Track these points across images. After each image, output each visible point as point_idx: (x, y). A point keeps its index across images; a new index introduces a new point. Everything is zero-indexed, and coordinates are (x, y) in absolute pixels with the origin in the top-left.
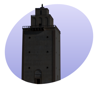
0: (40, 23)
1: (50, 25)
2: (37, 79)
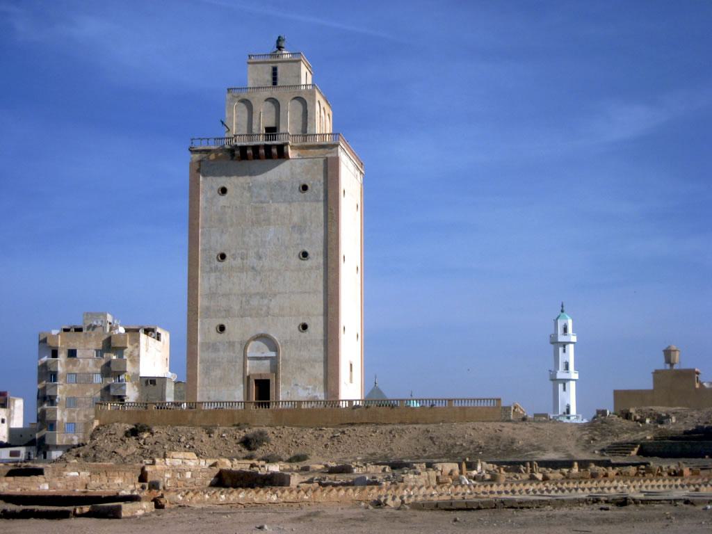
0: (271, 124)
1: (318, 131)
2: (257, 382)
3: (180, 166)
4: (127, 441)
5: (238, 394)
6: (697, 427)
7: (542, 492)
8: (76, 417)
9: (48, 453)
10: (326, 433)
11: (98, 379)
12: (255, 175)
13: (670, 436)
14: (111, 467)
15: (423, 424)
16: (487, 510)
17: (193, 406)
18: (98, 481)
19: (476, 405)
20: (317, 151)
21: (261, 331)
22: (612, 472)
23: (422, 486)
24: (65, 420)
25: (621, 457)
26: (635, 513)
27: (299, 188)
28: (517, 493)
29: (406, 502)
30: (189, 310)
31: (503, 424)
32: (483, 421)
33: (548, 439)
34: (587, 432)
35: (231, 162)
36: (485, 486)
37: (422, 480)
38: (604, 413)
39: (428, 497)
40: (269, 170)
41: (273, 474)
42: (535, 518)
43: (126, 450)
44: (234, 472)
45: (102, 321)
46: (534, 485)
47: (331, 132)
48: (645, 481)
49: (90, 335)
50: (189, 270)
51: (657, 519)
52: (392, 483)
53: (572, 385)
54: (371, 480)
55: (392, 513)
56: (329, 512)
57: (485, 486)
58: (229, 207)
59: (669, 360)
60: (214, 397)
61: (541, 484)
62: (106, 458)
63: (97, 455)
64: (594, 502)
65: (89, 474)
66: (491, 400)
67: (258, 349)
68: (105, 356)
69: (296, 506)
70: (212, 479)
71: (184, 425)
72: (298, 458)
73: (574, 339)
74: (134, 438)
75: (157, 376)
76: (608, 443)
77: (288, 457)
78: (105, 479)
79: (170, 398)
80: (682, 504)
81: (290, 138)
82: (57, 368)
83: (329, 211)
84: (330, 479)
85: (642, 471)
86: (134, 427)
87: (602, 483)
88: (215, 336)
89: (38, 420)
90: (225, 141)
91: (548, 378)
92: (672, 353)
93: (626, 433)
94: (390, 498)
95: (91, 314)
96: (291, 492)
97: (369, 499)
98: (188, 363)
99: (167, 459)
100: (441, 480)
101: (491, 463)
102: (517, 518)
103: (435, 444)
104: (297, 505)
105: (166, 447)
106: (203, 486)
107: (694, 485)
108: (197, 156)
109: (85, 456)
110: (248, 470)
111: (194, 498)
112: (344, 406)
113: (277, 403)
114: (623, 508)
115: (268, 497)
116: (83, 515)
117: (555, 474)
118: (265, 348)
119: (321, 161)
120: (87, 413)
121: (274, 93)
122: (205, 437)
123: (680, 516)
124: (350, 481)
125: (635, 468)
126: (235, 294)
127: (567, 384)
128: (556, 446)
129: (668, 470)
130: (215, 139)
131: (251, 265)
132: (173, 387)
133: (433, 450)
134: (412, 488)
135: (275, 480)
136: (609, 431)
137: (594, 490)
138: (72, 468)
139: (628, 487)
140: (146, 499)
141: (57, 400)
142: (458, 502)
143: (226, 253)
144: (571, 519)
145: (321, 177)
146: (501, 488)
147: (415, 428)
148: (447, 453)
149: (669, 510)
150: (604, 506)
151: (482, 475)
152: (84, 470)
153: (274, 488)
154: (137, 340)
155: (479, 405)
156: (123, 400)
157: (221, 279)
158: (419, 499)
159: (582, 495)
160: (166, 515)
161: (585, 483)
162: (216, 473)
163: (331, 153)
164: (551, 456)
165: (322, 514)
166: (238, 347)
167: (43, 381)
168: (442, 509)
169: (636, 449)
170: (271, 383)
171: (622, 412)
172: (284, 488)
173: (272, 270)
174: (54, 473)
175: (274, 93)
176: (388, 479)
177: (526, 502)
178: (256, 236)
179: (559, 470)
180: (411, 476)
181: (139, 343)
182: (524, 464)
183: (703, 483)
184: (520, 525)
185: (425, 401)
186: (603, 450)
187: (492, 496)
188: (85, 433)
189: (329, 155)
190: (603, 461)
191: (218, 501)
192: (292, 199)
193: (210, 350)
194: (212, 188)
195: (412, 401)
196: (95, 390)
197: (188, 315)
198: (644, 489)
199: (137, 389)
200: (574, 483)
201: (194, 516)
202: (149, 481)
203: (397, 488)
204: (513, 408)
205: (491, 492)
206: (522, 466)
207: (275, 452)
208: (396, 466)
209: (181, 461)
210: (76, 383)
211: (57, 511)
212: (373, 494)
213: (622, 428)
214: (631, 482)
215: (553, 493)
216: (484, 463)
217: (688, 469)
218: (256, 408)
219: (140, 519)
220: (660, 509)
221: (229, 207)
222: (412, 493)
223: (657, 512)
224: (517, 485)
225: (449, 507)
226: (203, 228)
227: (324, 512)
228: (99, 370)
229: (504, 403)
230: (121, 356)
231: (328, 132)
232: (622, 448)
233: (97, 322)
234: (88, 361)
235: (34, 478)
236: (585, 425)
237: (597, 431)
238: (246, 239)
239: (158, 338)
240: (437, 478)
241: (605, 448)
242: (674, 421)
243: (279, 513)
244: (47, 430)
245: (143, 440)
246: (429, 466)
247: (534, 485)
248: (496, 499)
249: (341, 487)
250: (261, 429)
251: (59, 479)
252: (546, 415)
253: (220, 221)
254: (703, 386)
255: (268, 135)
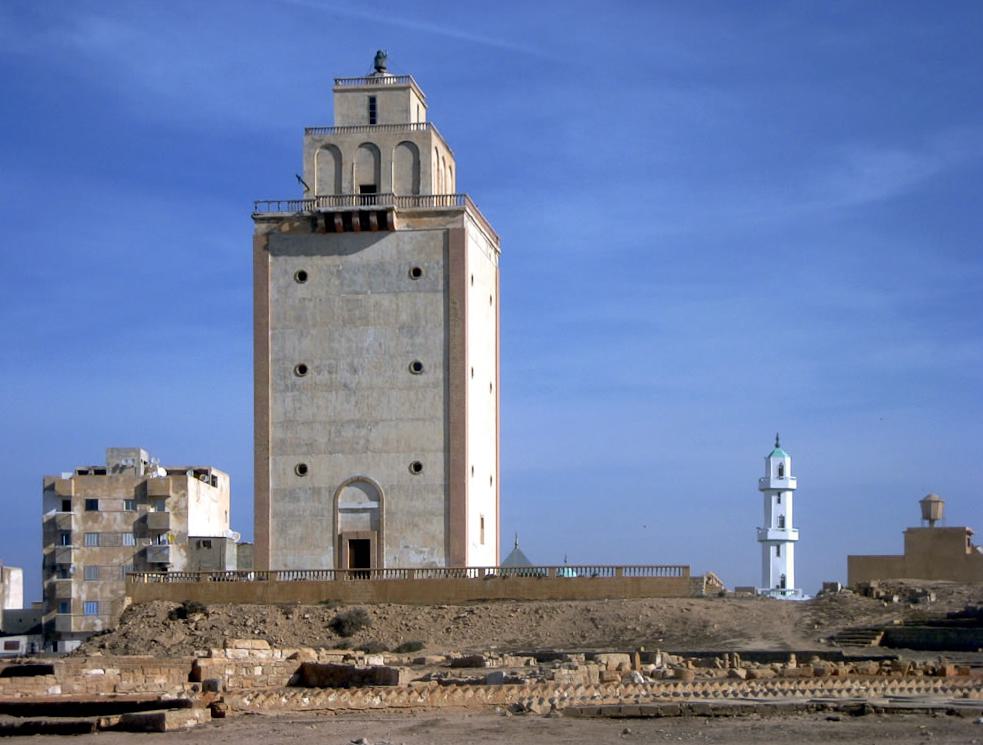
0: (369, 181)
1: (435, 192)
2: (353, 543)
3: (240, 241)
4: (171, 626)
5: (327, 560)
6: (967, 608)
7: (746, 694)
8: (99, 593)
9: (59, 644)
10: (447, 613)
11: (129, 540)
12: (347, 254)
13: (927, 620)
14: (150, 661)
15: (582, 600)
16: (669, 719)
17: (264, 576)
18: (131, 681)
19: (654, 575)
20: (433, 219)
21: (358, 473)
22: (844, 669)
23: (580, 685)
24: (84, 597)
25: (856, 649)
26: (876, 726)
27: (409, 273)
28: (711, 696)
29: (558, 707)
30: (256, 445)
31: (692, 601)
32: (664, 597)
33: (754, 622)
34: (809, 613)
35: (313, 235)
36: (667, 686)
37: (579, 677)
38: (833, 587)
39: (588, 700)
40: (366, 247)
41: (375, 669)
42: (736, 730)
43: (171, 637)
44: (322, 666)
45: (133, 460)
46: (735, 684)
47: (454, 192)
48: (890, 682)
49: (117, 480)
50: (256, 388)
51: (907, 735)
52: (538, 681)
53: (789, 548)
54: (510, 677)
55: (538, 722)
56: (452, 720)
57: (667, 686)
58: (310, 300)
59: (928, 516)
60: (294, 563)
61: (745, 684)
62: (142, 649)
63: (130, 645)
64: (818, 710)
65: (118, 672)
66: (675, 568)
67: (354, 497)
68: (138, 508)
69: (406, 712)
70: (291, 676)
71: (252, 603)
72: (409, 647)
73: (793, 484)
74: (181, 621)
75: (212, 535)
76: (838, 629)
77: (395, 645)
78: (141, 678)
79: (231, 566)
80: (944, 714)
81: (396, 201)
82: (70, 525)
83: (451, 305)
84: (453, 675)
85: (887, 668)
86: (181, 605)
87: (830, 684)
88: (292, 478)
89: (44, 599)
90: (304, 205)
91: (756, 539)
92: (933, 505)
93: (865, 615)
94: (535, 701)
95: (118, 450)
96: (400, 693)
97: (507, 702)
98: (256, 517)
99: (228, 650)
100: (605, 677)
101: (675, 654)
102: (711, 730)
103: (598, 628)
104: (408, 711)
105: (226, 633)
106: (278, 687)
107: (961, 690)
108: (263, 227)
109: (113, 647)
110: (340, 664)
111: (266, 703)
112: (473, 576)
113: (380, 571)
114: (859, 718)
115: (368, 700)
116: (110, 728)
117: (766, 671)
118: (364, 496)
119: (440, 234)
120: (115, 587)
121: (372, 135)
122: (281, 619)
123: (941, 732)
124: (481, 678)
125: (877, 663)
126: (320, 422)
127: (781, 547)
128: (766, 631)
129: (923, 667)
130: (289, 202)
131: (343, 381)
132: (235, 550)
133: (596, 635)
134: (566, 688)
135: (377, 677)
136: (841, 613)
137: (818, 693)
138: (94, 663)
139: (867, 690)
140: (199, 705)
141: (71, 570)
142: (628, 707)
143: (306, 364)
144: (786, 733)
145: (440, 257)
146: (689, 688)
147: (570, 606)
148: (613, 640)
149: (924, 723)
150: (833, 714)
151: (662, 670)
152: (111, 666)
153: (376, 687)
154: (184, 486)
155: (659, 575)
156: (166, 569)
157: (300, 401)
158: (576, 702)
159: (801, 699)
160: (228, 726)
161: (806, 683)
162: (296, 668)
163: (453, 222)
164: (758, 645)
165: (443, 723)
166: (325, 497)
167: (49, 544)
168: (607, 717)
169: (879, 638)
170: (371, 543)
171: (859, 586)
172: (391, 687)
173: (371, 388)
174: (68, 671)
175: (372, 135)
176: (533, 675)
177: (723, 708)
178: (349, 340)
179: (769, 665)
180: (565, 671)
181: (187, 490)
182: (721, 655)
183: (975, 687)
184: (716, 739)
185: (584, 569)
186: (831, 638)
187: (676, 699)
188: (112, 615)
189: (450, 226)
190: (831, 653)
191: (299, 707)
192: (399, 288)
193: (287, 499)
194: (286, 272)
195: (566, 570)
196: (125, 555)
197: (255, 452)
198: (889, 692)
199: (184, 554)
200: (791, 683)
201: (267, 727)
202: (203, 679)
203: (545, 688)
204: (705, 580)
205: (676, 694)
206: (718, 659)
207: (377, 639)
208: (545, 657)
209: (247, 652)
210: (98, 545)
211: (73, 724)
212: (513, 695)
213: (858, 608)
214: (871, 683)
215: (761, 696)
216: (665, 654)
217: (953, 666)
218: (351, 579)
219: (190, 732)
220: (911, 721)
221: (310, 300)
222: (566, 695)
223: (907, 724)
224: (711, 684)
225: (617, 714)
226: (273, 329)
227: (444, 720)
228: (131, 528)
229: (693, 573)
230: (161, 508)
231: (449, 193)
232: (860, 636)
233: (127, 461)
234: (115, 515)
235: (40, 678)
236: (806, 603)
237: (822, 611)
238: (336, 345)
239: (214, 482)
240: (601, 674)
241: (835, 635)
242: (933, 599)
243: (383, 722)
244: (58, 612)
245: (194, 624)
246: (590, 657)
247: (735, 684)
248: (681, 703)
249: (468, 686)
250: (358, 607)
251: (76, 680)
252: (752, 590)
253: (298, 319)
254: (978, 551)
255: (364, 197)
